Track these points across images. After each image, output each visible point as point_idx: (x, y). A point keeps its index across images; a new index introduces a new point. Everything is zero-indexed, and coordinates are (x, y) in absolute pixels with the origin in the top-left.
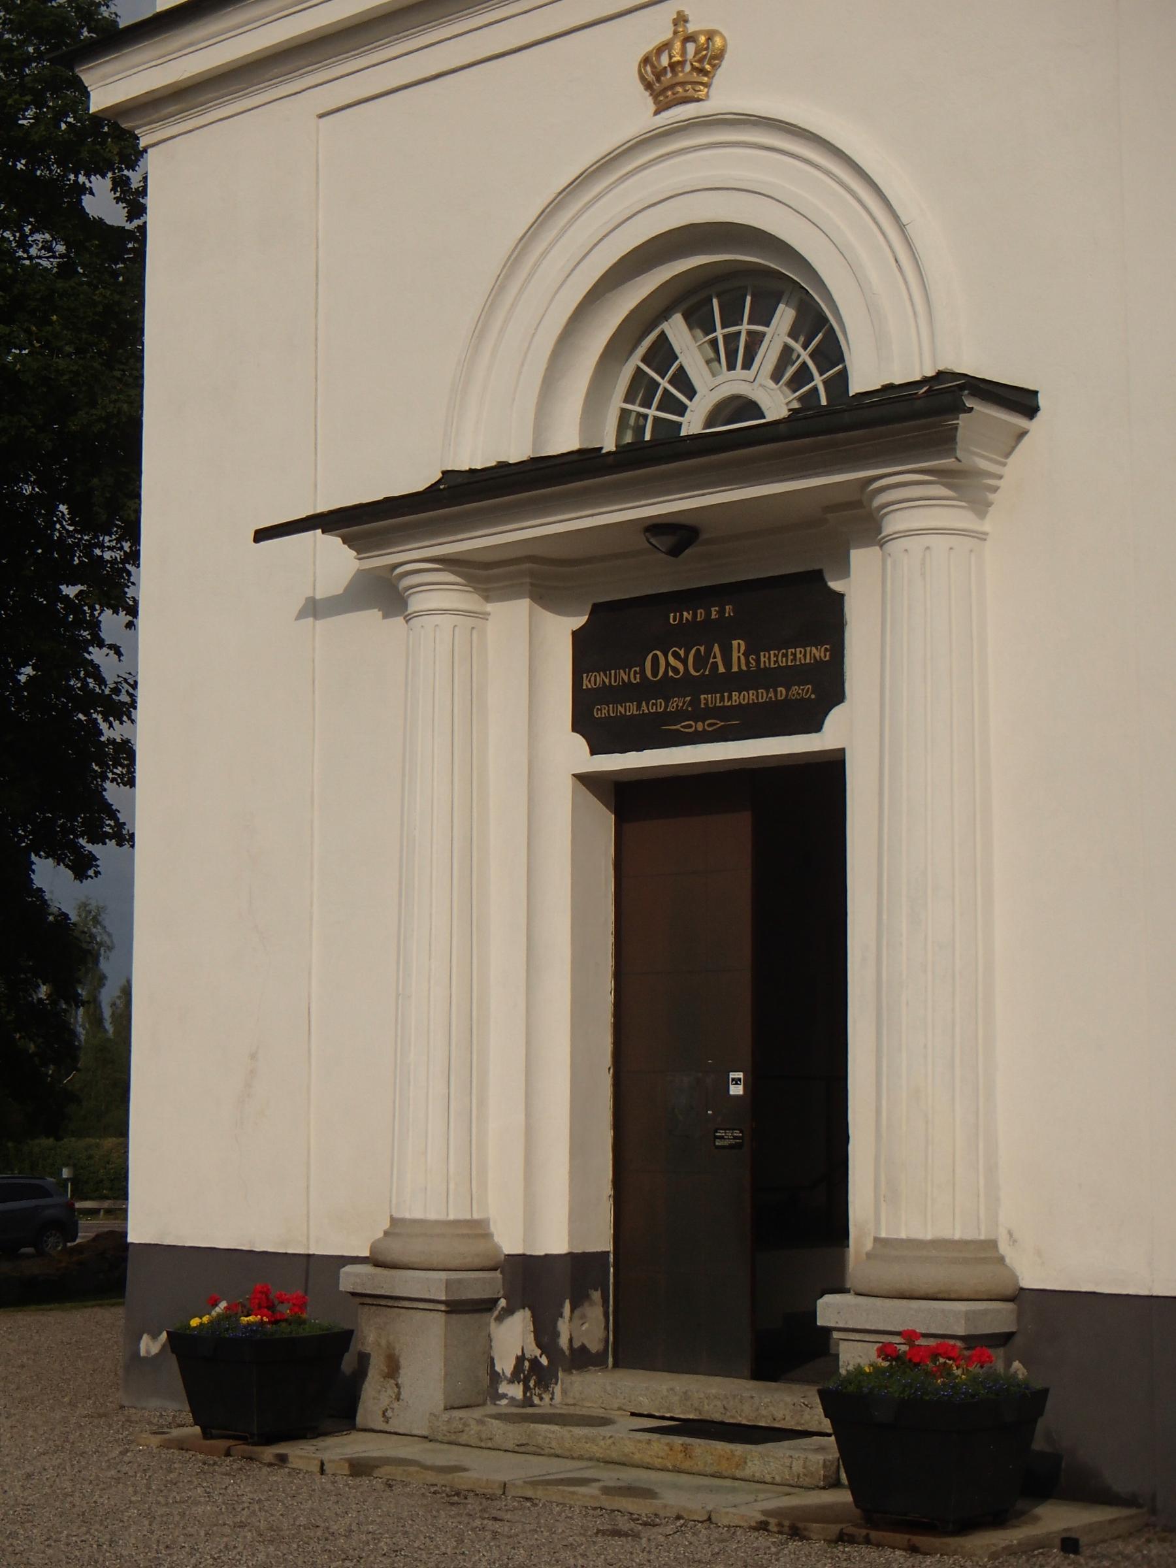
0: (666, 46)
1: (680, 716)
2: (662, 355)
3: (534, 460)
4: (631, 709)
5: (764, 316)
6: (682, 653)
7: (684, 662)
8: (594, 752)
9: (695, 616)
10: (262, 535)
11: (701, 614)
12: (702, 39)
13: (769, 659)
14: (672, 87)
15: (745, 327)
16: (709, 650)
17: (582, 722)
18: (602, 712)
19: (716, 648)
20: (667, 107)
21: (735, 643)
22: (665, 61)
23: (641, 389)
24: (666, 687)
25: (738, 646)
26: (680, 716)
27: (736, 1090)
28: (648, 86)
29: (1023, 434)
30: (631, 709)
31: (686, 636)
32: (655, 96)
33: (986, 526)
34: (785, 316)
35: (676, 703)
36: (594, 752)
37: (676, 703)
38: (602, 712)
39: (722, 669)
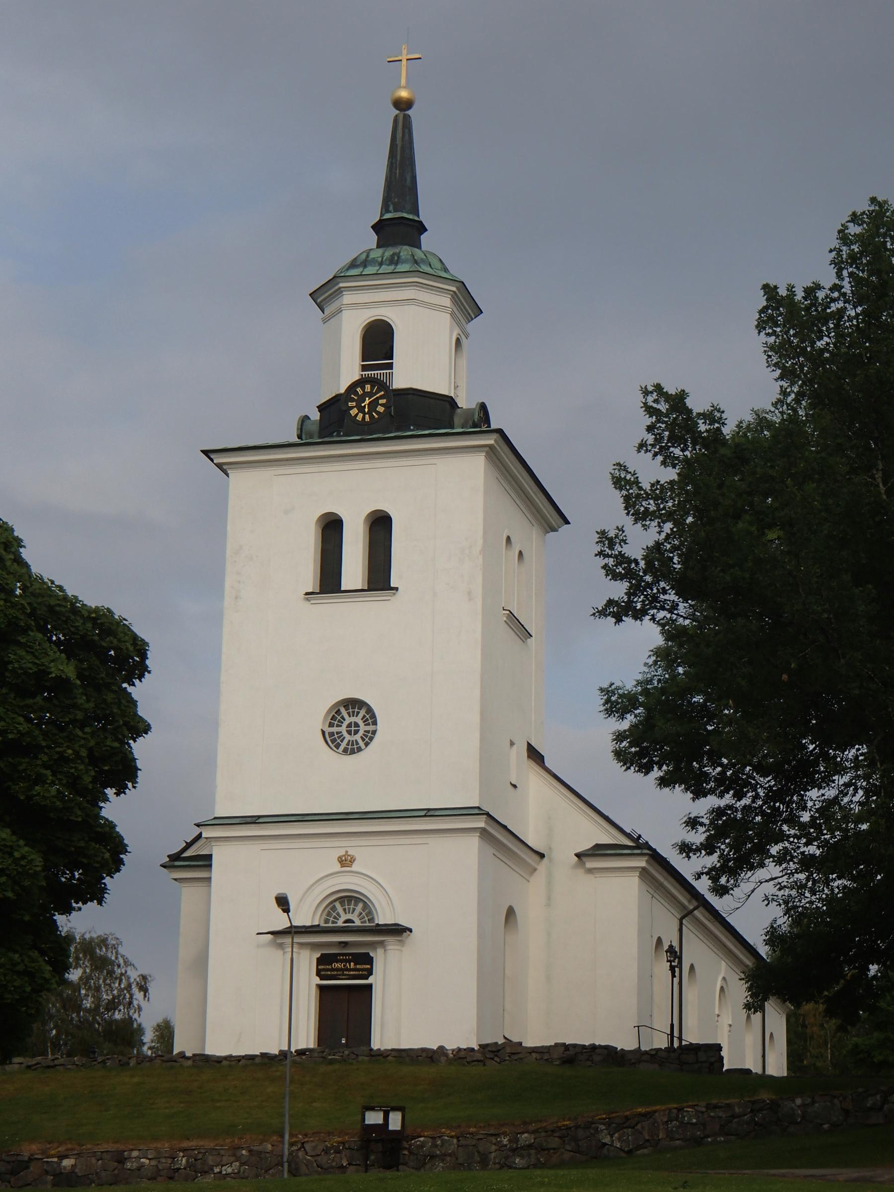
0: (344, 856)
1: (340, 975)
2: (334, 909)
4: (329, 973)
5: (356, 905)
8: (321, 980)
10: (258, 934)
13: (358, 966)
17: (318, 974)
18: (323, 973)
22: (343, 858)
23: (329, 914)
24: (337, 970)
25: (352, 964)
26: (340, 975)
27: (343, 1042)
29: (409, 935)
30: (329, 973)
31: (341, 961)
32: (341, 865)
33: (403, 949)
34: (360, 905)
35: (339, 973)
36: (321, 980)
37: (339, 973)
38: (323, 973)
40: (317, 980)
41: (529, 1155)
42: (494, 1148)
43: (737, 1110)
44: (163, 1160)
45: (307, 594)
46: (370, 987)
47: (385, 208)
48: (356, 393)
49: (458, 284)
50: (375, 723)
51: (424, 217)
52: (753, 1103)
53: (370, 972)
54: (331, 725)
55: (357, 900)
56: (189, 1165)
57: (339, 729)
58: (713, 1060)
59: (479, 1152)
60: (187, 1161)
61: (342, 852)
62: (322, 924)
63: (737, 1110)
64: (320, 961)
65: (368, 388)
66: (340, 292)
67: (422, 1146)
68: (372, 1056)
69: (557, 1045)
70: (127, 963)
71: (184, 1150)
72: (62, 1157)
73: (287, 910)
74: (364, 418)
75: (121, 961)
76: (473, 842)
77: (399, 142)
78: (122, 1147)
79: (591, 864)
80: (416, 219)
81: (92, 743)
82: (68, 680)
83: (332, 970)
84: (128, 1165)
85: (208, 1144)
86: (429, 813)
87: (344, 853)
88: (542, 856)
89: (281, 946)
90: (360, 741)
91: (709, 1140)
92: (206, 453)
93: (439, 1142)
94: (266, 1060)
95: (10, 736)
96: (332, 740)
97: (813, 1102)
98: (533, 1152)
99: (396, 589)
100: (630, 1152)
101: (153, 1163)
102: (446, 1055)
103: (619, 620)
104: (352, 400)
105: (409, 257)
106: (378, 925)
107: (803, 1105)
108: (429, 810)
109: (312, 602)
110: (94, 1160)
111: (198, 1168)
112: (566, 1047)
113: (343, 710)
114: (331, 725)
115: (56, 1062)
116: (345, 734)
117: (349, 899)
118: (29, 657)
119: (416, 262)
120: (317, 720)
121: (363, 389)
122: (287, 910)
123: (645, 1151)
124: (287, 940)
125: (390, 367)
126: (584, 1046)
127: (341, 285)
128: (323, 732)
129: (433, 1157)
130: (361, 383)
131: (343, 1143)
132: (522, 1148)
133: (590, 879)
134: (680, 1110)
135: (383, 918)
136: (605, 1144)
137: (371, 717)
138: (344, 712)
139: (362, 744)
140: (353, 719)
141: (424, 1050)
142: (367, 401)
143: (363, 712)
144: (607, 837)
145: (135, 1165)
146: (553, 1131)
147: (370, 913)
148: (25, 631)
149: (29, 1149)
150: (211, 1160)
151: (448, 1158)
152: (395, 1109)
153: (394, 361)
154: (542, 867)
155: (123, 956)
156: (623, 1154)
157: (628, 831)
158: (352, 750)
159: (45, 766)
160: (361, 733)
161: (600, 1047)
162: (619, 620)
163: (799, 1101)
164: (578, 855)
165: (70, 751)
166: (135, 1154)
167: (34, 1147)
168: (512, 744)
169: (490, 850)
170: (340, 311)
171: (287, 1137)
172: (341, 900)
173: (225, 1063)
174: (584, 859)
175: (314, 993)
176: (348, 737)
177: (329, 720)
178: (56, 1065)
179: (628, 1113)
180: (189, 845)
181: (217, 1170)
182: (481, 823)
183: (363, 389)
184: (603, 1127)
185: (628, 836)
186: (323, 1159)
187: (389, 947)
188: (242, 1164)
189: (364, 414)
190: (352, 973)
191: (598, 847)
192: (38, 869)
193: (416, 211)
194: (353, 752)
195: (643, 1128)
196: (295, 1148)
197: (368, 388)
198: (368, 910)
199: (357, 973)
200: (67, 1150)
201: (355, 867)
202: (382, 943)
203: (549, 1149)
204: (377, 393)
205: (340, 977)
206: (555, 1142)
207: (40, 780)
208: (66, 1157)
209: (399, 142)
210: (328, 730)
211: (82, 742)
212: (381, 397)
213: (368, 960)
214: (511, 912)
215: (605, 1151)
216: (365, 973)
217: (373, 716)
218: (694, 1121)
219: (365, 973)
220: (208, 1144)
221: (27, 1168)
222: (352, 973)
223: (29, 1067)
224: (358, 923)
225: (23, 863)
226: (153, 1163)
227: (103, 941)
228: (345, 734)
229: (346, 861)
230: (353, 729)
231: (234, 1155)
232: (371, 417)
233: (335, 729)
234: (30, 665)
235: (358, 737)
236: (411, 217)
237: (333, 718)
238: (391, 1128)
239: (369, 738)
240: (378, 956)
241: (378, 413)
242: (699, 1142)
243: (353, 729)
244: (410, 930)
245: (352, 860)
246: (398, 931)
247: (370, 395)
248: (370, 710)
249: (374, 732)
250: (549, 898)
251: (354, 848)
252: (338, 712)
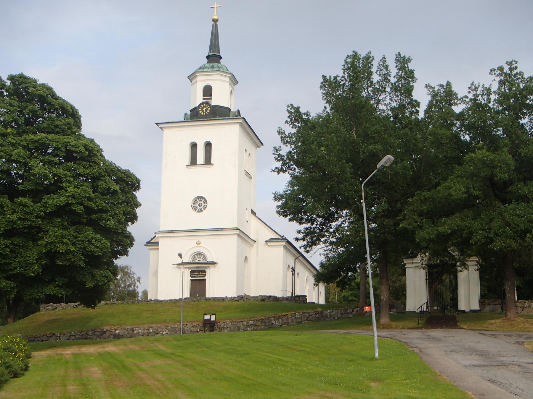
2: (195, 257)
17: (190, 276)
23: (193, 259)
24: (196, 275)
31: (197, 272)
34: (203, 256)
40: (190, 278)
41: (252, 327)
42: (241, 325)
43: (311, 314)
44: (146, 330)
45: (187, 165)
46: (205, 280)
47: (210, 51)
48: (201, 106)
49: (232, 75)
50: (207, 203)
51: (221, 54)
52: (316, 311)
53: (205, 275)
54: (194, 204)
55: (202, 255)
56: (153, 332)
57: (196, 205)
58: (304, 299)
59: (237, 326)
60: (153, 330)
62: (192, 262)
63: (311, 314)
64: (191, 272)
65: (205, 105)
66: (196, 76)
67: (221, 325)
68: (206, 299)
69: (259, 296)
70: (134, 273)
71: (151, 327)
72: (116, 330)
73: (181, 258)
74: (203, 114)
75: (132, 273)
76: (236, 237)
77: (214, 32)
78: (133, 327)
79: (269, 244)
80: (219, 55)
81: (124, 209)
82: (117, 191)
83: (194, 275)
84: (135, 332)
85: (159, 325)
86: (222, 229)
88: (255, 241)
89: (179, 268)
90: (202, 209)
91: (303, 322)
92: (157, 124)
93: (226, 324)
94: (176, 301)
95: (100, 207)
96: (194, 208)
97: (333, 311)
98: (253, 326)
99: (213, 164)
100: (281, 326)
101: (143, 331)
102: (228, 299)
103: (279, 173)
104: (200, 108)
105: (217, 66)
106: (208, 262)
107: (330, 312)
108: (223, 228)
110: (125, 331)
111: (156, 333)
112: (262, 296)
113: (197, 199)
114: (194, 204)
115: (114, 302)
116: (198, 206)
117: (199, 254)
118: (105, 184)
119: (219, 68)
120: (190, 202)
121: (203, 105)
122: (181, 258)
123: (285, 326)
124: (182, 266)
125: (211, 99)
126: (267, 296)
127: (197, 74)
128: (192, 206)
129: (224, 328)
130: (203, 103)
131: (198, 324)
132: (250, 325)
133: (269, 248)
134: (295, 314)
135: (209, 260)
136: (273, 324)
137: (205, 202)
138: (198, 200)
139: (203, 209)
140: (200, 202)
141: (221, 297)
142: (204, 109)
143: (203, 200)
144: (274, 236)
145: (137, 332)
146: (258, 320)
147: (205, 258)
148: (104, 176)
149: (105, 328)
150: (159, 330)
151: (228, 328)
152: (213, 314)
153: (213, 97)
154: (255, 245)
155: (132, 271)
156: (278, 327)
157: (280, 234)
158: (200, 211)
159: (110, 216)
160: (203, 206)
161: (272, 296)
162: (279, 173)
163: (328, 311)
164: (266, 241)
165: (118, 212)
166: (137, 329)
167: (107, 327)
168: (247, 209)
169: (240, 240)
170: (196, 82)
171: (182, 323)
172: (197, 255)
173: (163, 302)
174: (267, 242)
175: (189, 282)
176: (199, 207)
177: (193, 202)
178: (113, 304)
179: (280, 315)
180: (152, 239)
181: (161, 333)
182: (238, 232)
183: (203, 105)
184: (273, 319)
185: (280, 236)
186: (192, 329)
187: (211, 268)
188: (169, 331)
189: (204, 112)
191: (271, 239)
192: (108, 246)
193: (219, 52)
194: (200, 212)
195: (284, 319)
196: (184, 326)
197: (205, 105)
198: (205, 258)
200: (117, 328)
201: (201, 245)
202: (209, 267)
203: (257, 325)
204: (207, 106)
206: (259, 323)
207: (109, 220)
208: (117, 330)
209: (214, 32)
210: (193, 205)
211: (121, 209)
212: (209, 108)
213: (204, 272)
214: (246, 258)
215: (273, 325)
217: (206, 201)
218: (299, 317)
220: (159, 325)
221: (106, 333)
223: (105, 304)
224: (202, 261)
225: (104, 244)
226: (143, 331)
227: (126, 267)
228: (198, 206)
229: (198, 243)
231: (166, 328)
232: (206, 113)
233: (195, 205)
234: (105, 186)
235: (202, 207)
236: (217, 54)
237: (195, 202)
238: (212, 320)
239: (205, 207)
240: (208, 271)
241: (208, 112)
242: (300, 323)
243: (200, 205)
244: (217, 263)
245: (200, 243)
246: (213, 263)
247: (205, 107)
248: (205, 200)
249: (206, 206)
250: (257, 254)
251: (202, 240)
252: (196, 200)
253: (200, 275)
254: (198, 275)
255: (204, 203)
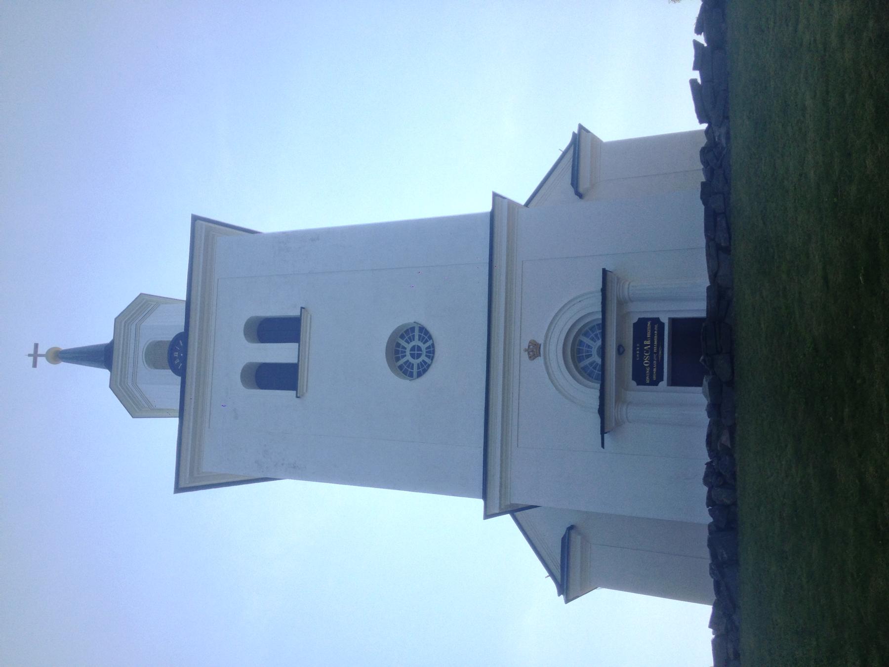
1: (657, 357)
3: (600, 390)
4: (655, 370)
6: (645, 357)
7: (647, 356)
9: (638, 347)
10: (603, 446)
11: (638, 352)
12: (530, 344)
13: (649, 335)
14: (537, 353)
15: (584, 348)
16: (645, 350)
17: (655, 383)
18: (654, 378)
19: (645, 348)
20: (540, 353)
21: (645, 343)
24: (651, 360)
28: (536, 357)
30: (655, 370)
38: (654, 378)
39: (649, 347)
40: (663, 384)
53: (656, 321)
61: (525, 355)
83: (651, 366)
87: (527, 353)
89: (619, 424)
109: (305, 391)
120: (403, 383)
140: (408, 353)
183: (175, 358)
190: (656, 343)
191: (572, 184)
199: (656, 337)
201: (541, 341)
202: (621, 303)
205: (660, 357)
213: (641, 326)
216: (656, 326)
219: (656, 326)
222: (656, 343)
228: (420, 360)
229: (534, 350)
230: (416, 352)
253: (652, 348)
254: (651, 356)
255: (412, 339)
